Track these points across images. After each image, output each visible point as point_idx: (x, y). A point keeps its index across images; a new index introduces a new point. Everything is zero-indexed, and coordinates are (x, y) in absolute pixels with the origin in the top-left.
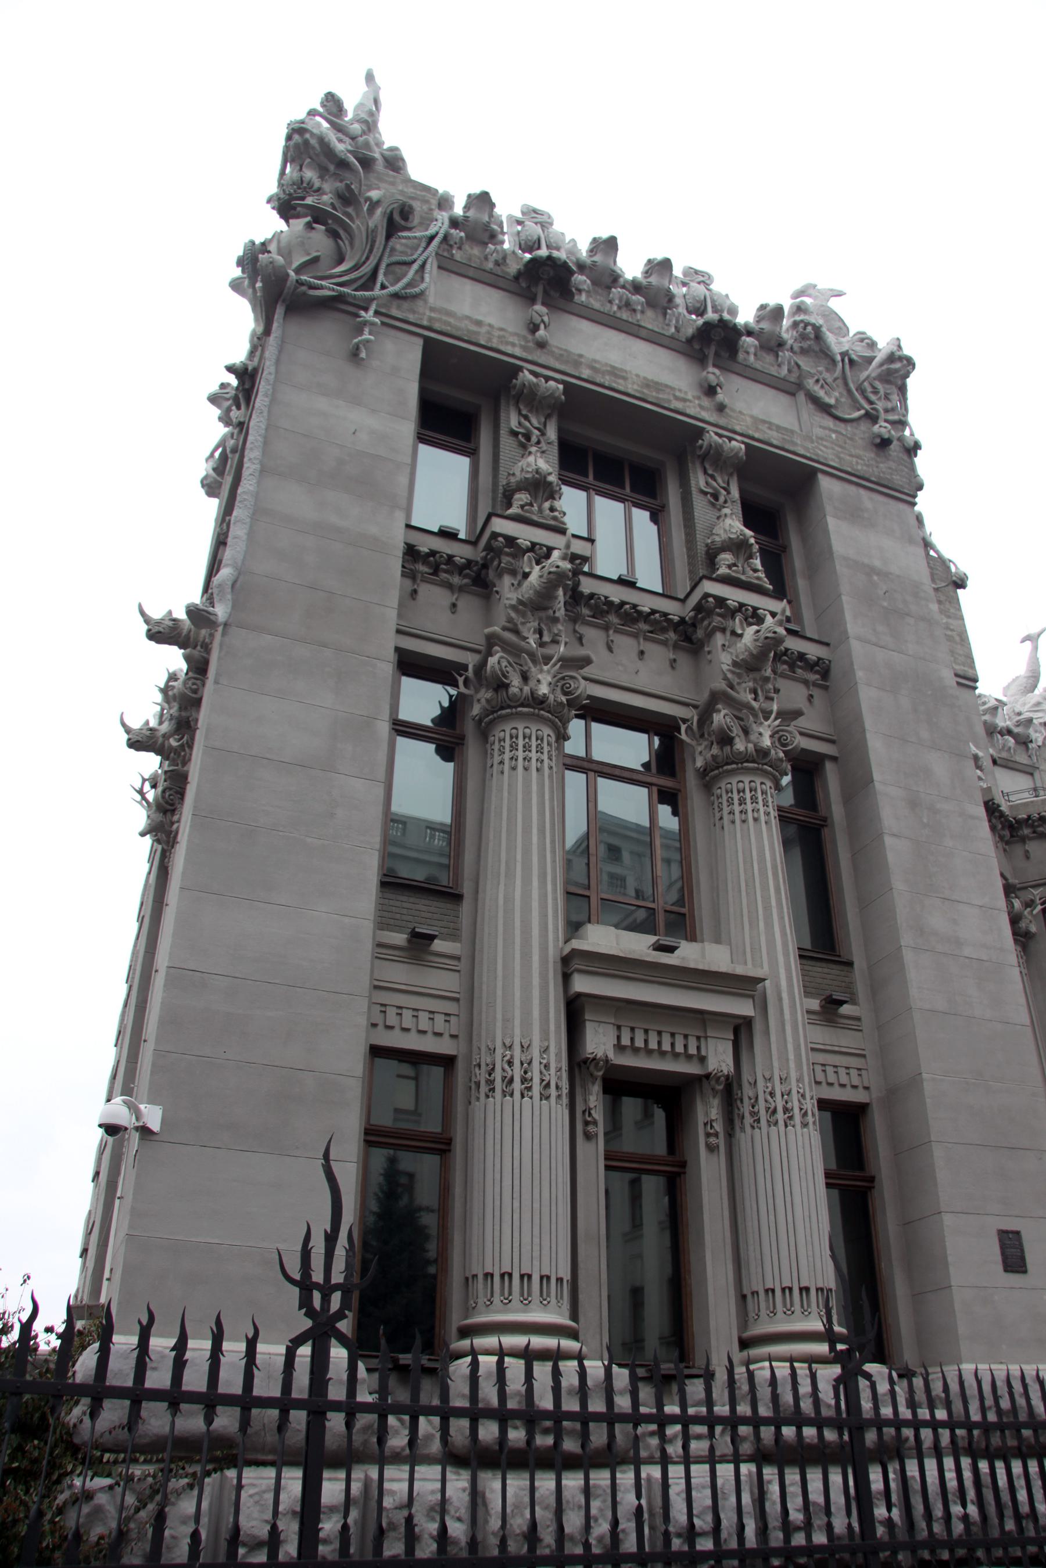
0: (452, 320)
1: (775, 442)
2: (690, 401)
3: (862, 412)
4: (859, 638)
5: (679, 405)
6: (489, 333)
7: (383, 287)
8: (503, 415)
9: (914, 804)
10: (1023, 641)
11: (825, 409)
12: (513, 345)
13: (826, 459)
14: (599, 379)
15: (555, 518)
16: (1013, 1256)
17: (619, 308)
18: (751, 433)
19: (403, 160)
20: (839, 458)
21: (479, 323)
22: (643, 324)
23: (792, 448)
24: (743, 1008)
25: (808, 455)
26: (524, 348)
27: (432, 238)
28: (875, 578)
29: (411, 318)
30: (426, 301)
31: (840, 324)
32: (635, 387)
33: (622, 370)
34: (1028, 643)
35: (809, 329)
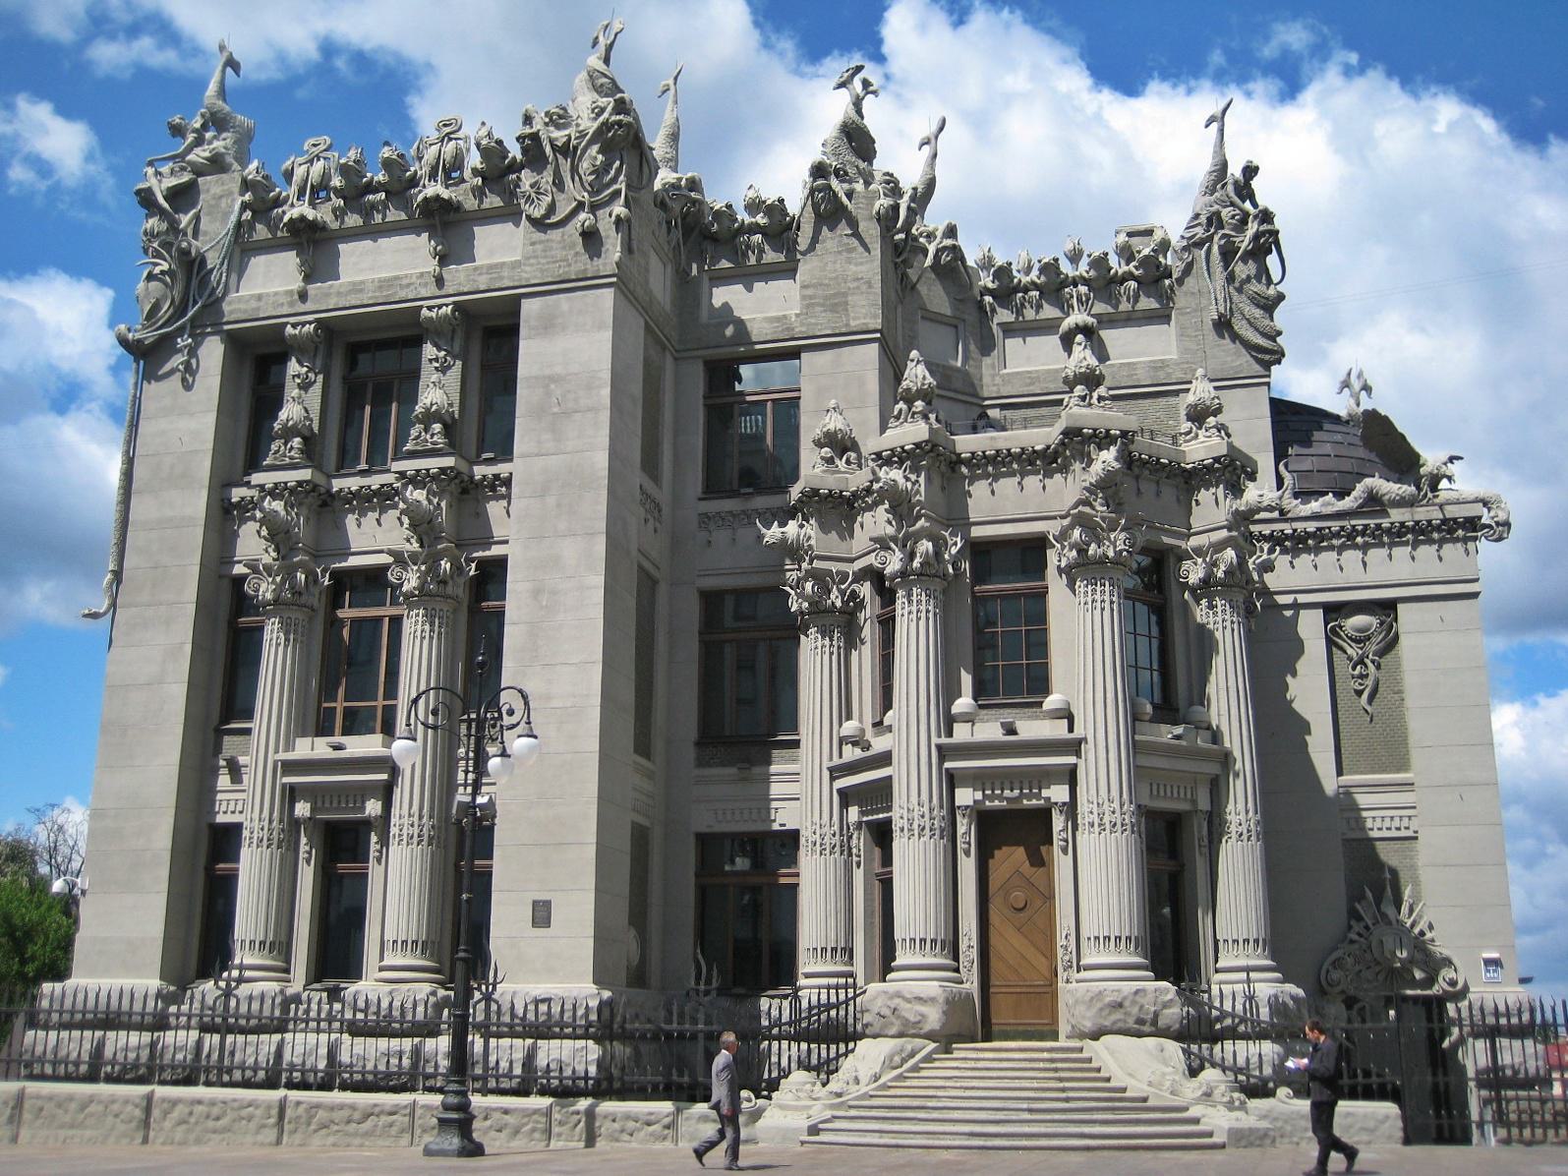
0: (242, 306)
1: (482, 288)
3: (574, 204)
4: (523, 456)
5: (402, 294)
7: (195, 302)
9: (536, 593)
10: (1207, 126)
11: (539, 224)
12: (282, 304)
13: (528, 279)
15: (291, 458)
16: (542, 915)
20: (542, 271)
21: (259, 297)
23: (497, 286)
24: (385, 776)
25: (511, 284)
26: (291, 304)
28: (553, 386)
33: (362, 282)
34: (1215, 126)
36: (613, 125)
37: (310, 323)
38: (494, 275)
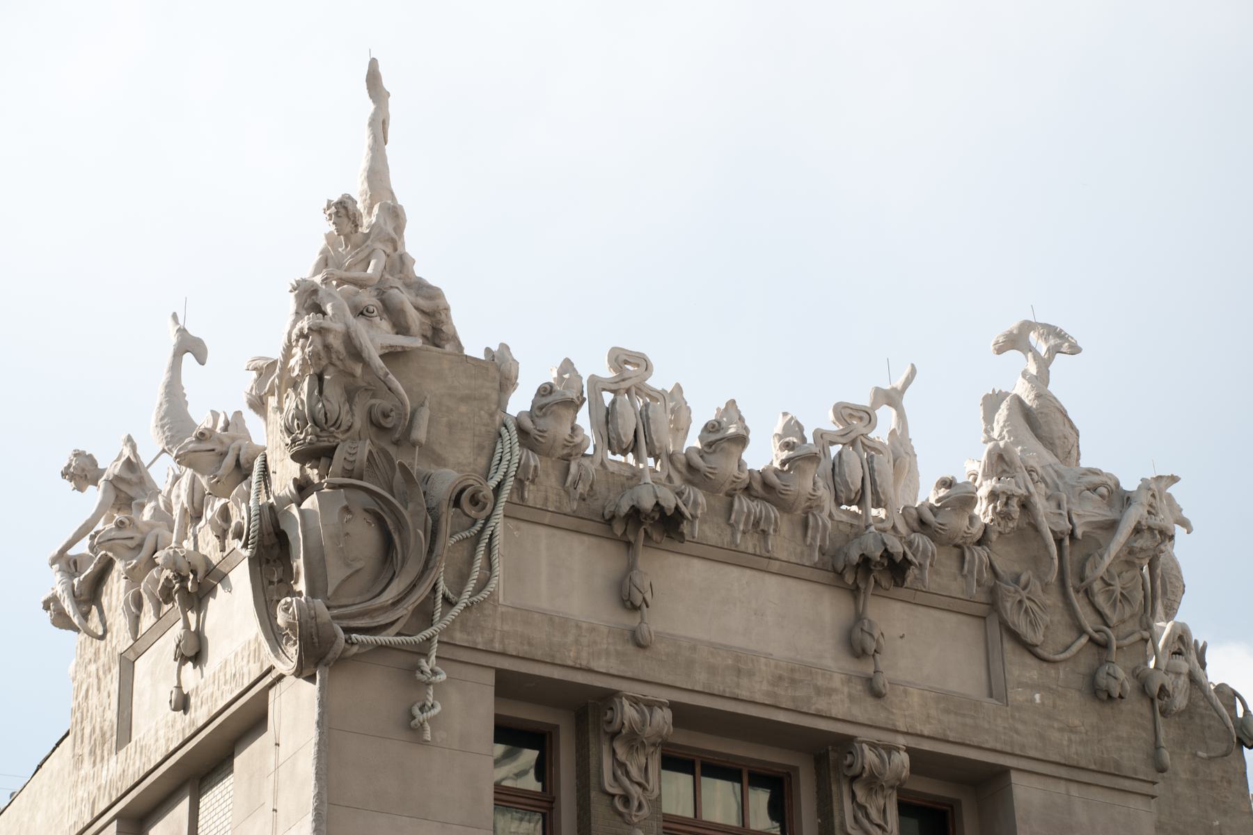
1: (952, 736)
2: (835, 690)
3: (1084, 640)
5: (821, 704)
6: (577, 642)
8: (593, 749)
11: (1029, 648)
14: (717, 688)
17: (744, 533)
18: (919, 728)
19: (447, 309)
20: (1042, 737)
22: (776, 555)
23: (975, 741)
25: (999, 747)
27: (500, 485)
29: (480, 642)
30: (496, 604)
31: (1068, 430)
32: (765, 687)
35: (1014, 503)
36: (1150, 529)
37: (661, 705)
38: (969, 721)
